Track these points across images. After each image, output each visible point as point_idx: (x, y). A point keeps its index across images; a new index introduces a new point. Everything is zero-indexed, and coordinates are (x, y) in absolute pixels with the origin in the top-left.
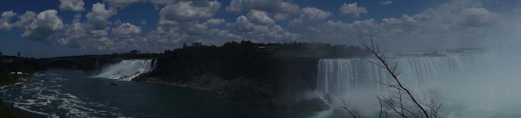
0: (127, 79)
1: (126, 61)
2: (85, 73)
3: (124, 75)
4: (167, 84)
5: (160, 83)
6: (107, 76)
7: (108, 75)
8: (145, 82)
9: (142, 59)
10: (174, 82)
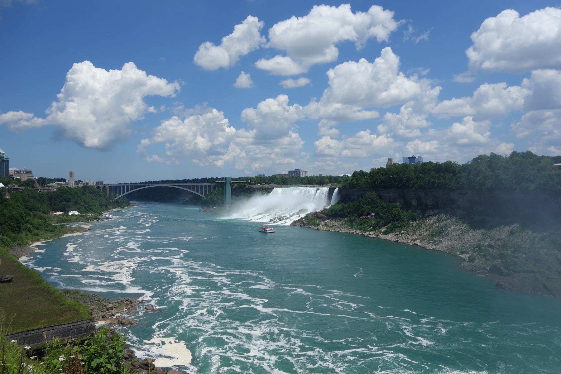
0: (282, 222)
1: (281, 189)
2: (204, 211)
4: (358, 234)
5: (343, 231)
6: (247, 217)
8: (316, 228)
9: (311, 187)
10: (371, 230)
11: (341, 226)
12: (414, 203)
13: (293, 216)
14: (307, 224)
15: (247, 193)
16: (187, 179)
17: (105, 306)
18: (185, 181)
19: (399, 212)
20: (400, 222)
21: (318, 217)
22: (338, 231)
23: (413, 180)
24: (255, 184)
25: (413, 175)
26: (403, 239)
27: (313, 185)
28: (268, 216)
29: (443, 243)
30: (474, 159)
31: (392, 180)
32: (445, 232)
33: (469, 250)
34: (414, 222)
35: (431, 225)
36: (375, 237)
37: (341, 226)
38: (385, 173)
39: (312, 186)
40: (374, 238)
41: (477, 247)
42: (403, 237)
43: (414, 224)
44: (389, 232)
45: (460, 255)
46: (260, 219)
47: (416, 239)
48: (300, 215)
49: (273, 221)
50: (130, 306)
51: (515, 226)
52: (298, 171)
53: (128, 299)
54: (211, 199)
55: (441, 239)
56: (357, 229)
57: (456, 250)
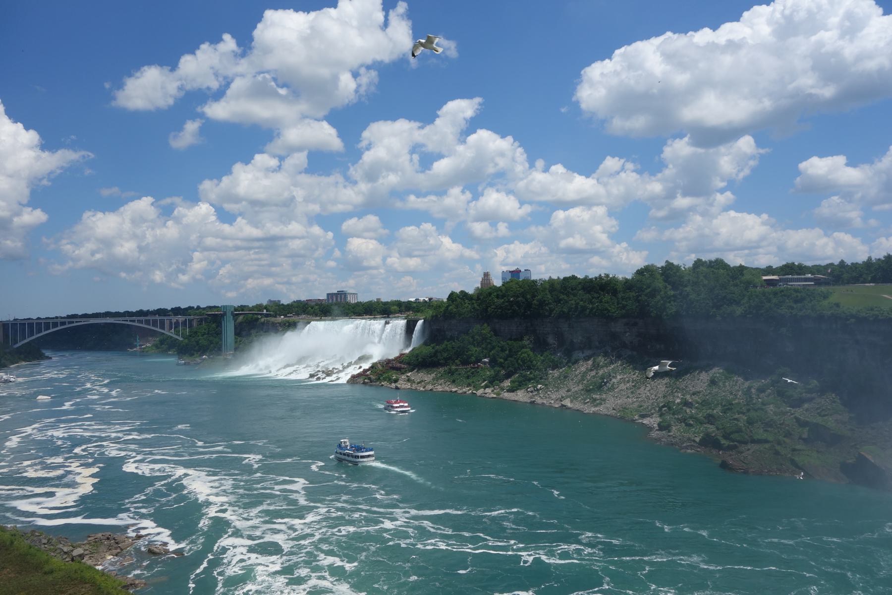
0: (333, 377)
1: (323, 323)
2: (185, 364)
3: (321, 364)
4: (465, 392)
5: (439, 388)
6: (267, 371)
7: (267, 367)
8: (393, 385)
9: (371, 319)
10: (486, 387)
11: (435, 382)
12: (551, 340)
13: (350, 368)
14: (375, 379)
15: (262, 330)
16: (145, 309)
17: (65, 553)
18: (141, 313)
19: (528, 355)
20: (533, 372)
21: (393, 368)
22: (431, 390)
23: (549, 304)
24: (275, 317)
25: (549, 296)
26: (541, 398)
27: (373, 317)
28: (304, 368)
29: (608, 402)
30: (638, 271)
31: (514, 306)
32: (608, 384)
33: (653, 411)
34: (555, 371)
35: (584, 375)
36: (495, 398)
37: (435, 382)
38: (501, 294)
39: (371, 317)
40: (494, 399)
41: (664, 406)
42: (542, 396)
43: (556, 373)
44: (516, 387)
45: (640, 420)
46: (292, 374)
47: (562, 397)
48: (361, 365)
49: (316, 377)
50: (116, 549)
51: (717, 371)
52: (343, 294)
53: (110, 535)
54: (197, 342)
55: (604, 396)
56: (462, 384)
57: (631, 412)
